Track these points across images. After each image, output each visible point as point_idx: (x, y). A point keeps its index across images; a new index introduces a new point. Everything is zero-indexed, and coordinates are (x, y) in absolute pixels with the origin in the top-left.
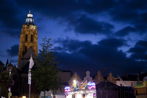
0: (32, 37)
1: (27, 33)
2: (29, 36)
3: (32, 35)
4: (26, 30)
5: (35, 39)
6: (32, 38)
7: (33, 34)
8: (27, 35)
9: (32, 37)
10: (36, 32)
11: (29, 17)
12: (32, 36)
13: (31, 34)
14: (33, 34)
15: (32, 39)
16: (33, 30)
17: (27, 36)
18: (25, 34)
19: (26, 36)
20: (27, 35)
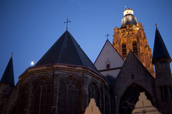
0: (136, 45)
1: (124, 40)
2: (129, 45)
3: (136, 43)
4: (121, 36)
5: (141, 48)
6: (136, 47)
7: (136, 39)
8: (124, 46)
9: (135, 46)
10: (140, 34)
11: (126, 15)
12: (135, 44)
13: (133, 40)
14: (136, 39)
15: (136, 49)
16: (136, 33)
17: (125, 47)
18: (121, 43)
19: (123, 47)
20: (125, 45)
